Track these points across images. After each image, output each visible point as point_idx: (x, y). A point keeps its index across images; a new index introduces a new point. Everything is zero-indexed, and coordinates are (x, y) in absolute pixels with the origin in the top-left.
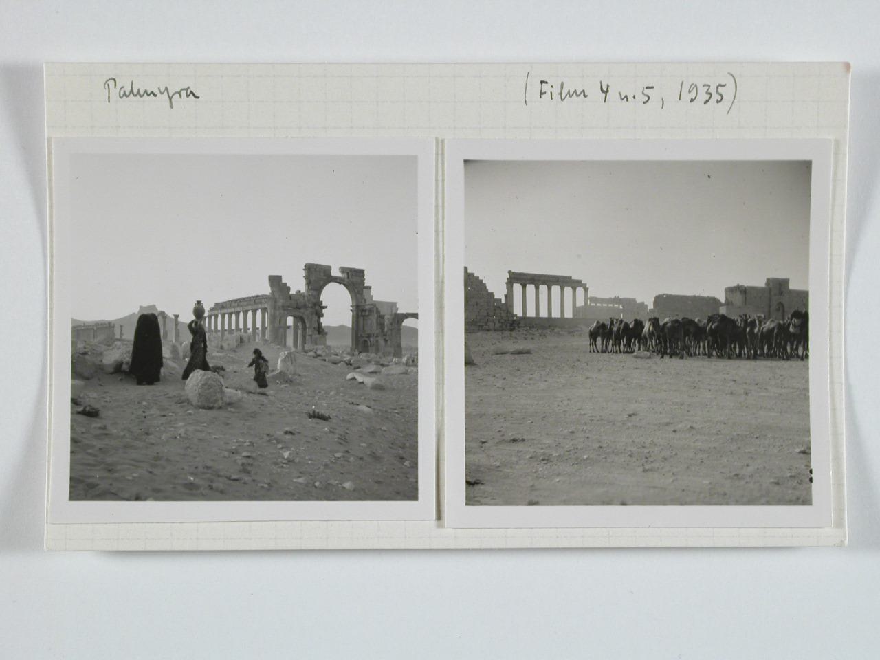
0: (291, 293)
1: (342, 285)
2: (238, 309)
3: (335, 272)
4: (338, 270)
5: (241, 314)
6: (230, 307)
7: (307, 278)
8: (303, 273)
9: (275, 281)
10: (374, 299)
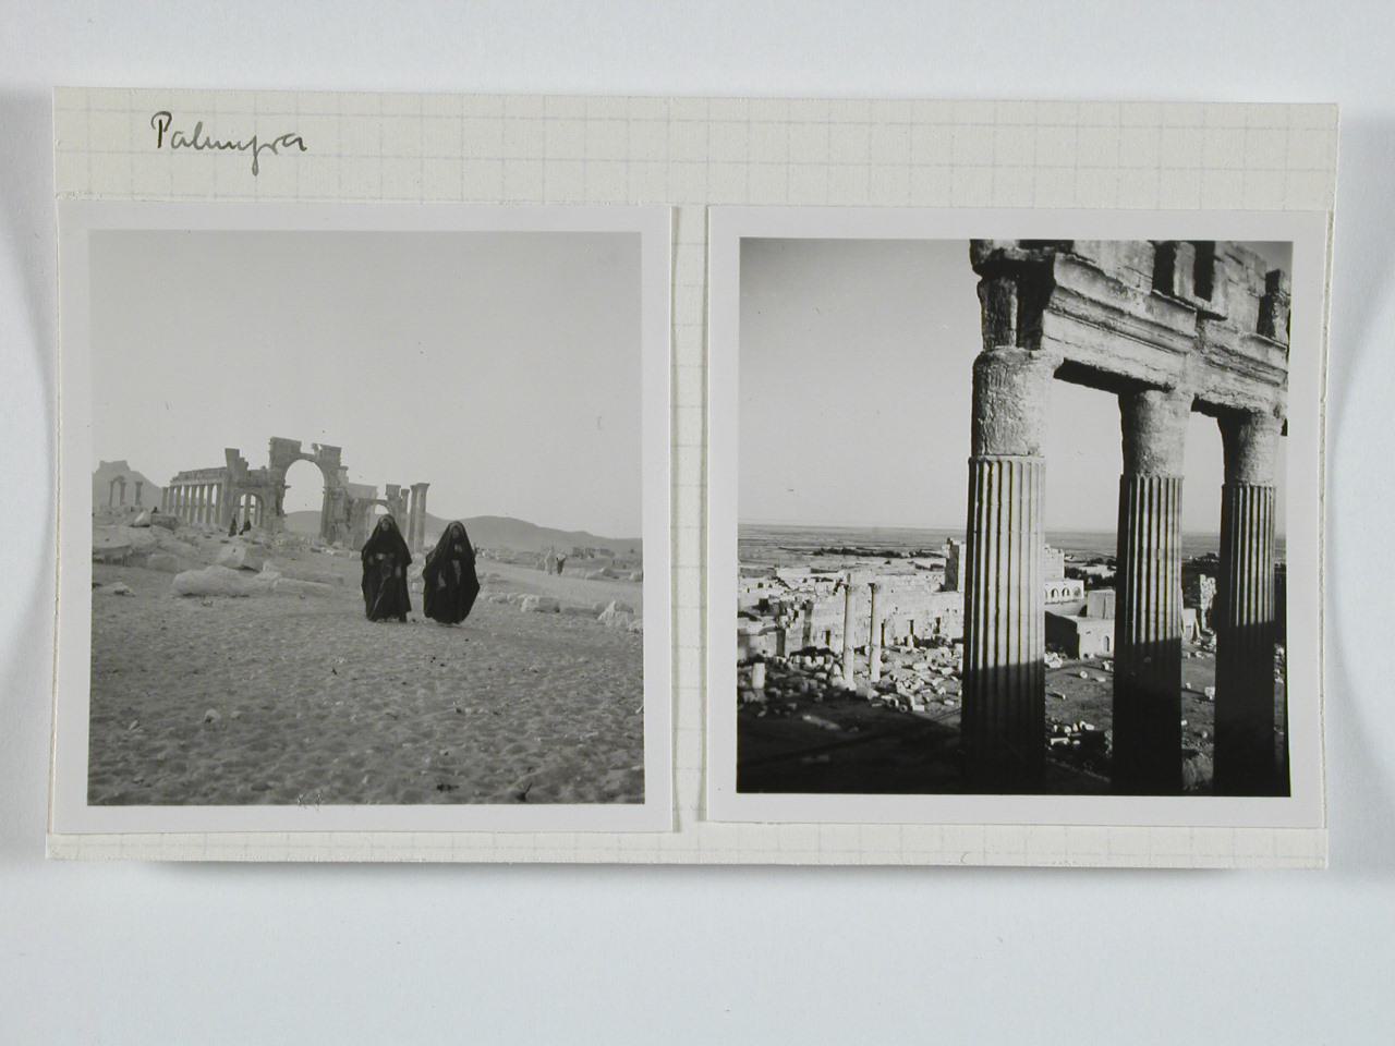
0: (249, 468)
1: (314, 464)
2: (203, 482)
3: (306, 449)
4: (310, 446)
5: (206, 488)
6: (195, 478)
7: (272, 453)
8: (268, 448)
9: (232, 454)
10: (350, 481)
